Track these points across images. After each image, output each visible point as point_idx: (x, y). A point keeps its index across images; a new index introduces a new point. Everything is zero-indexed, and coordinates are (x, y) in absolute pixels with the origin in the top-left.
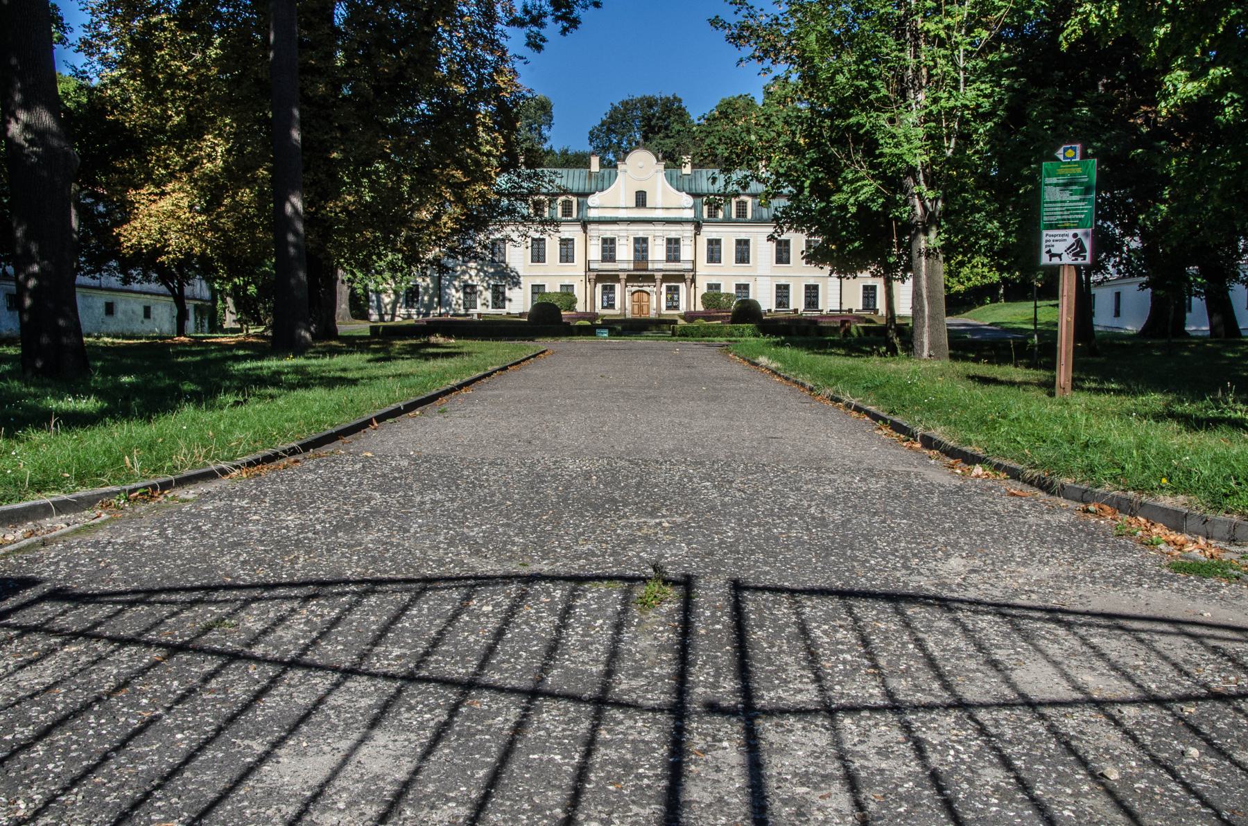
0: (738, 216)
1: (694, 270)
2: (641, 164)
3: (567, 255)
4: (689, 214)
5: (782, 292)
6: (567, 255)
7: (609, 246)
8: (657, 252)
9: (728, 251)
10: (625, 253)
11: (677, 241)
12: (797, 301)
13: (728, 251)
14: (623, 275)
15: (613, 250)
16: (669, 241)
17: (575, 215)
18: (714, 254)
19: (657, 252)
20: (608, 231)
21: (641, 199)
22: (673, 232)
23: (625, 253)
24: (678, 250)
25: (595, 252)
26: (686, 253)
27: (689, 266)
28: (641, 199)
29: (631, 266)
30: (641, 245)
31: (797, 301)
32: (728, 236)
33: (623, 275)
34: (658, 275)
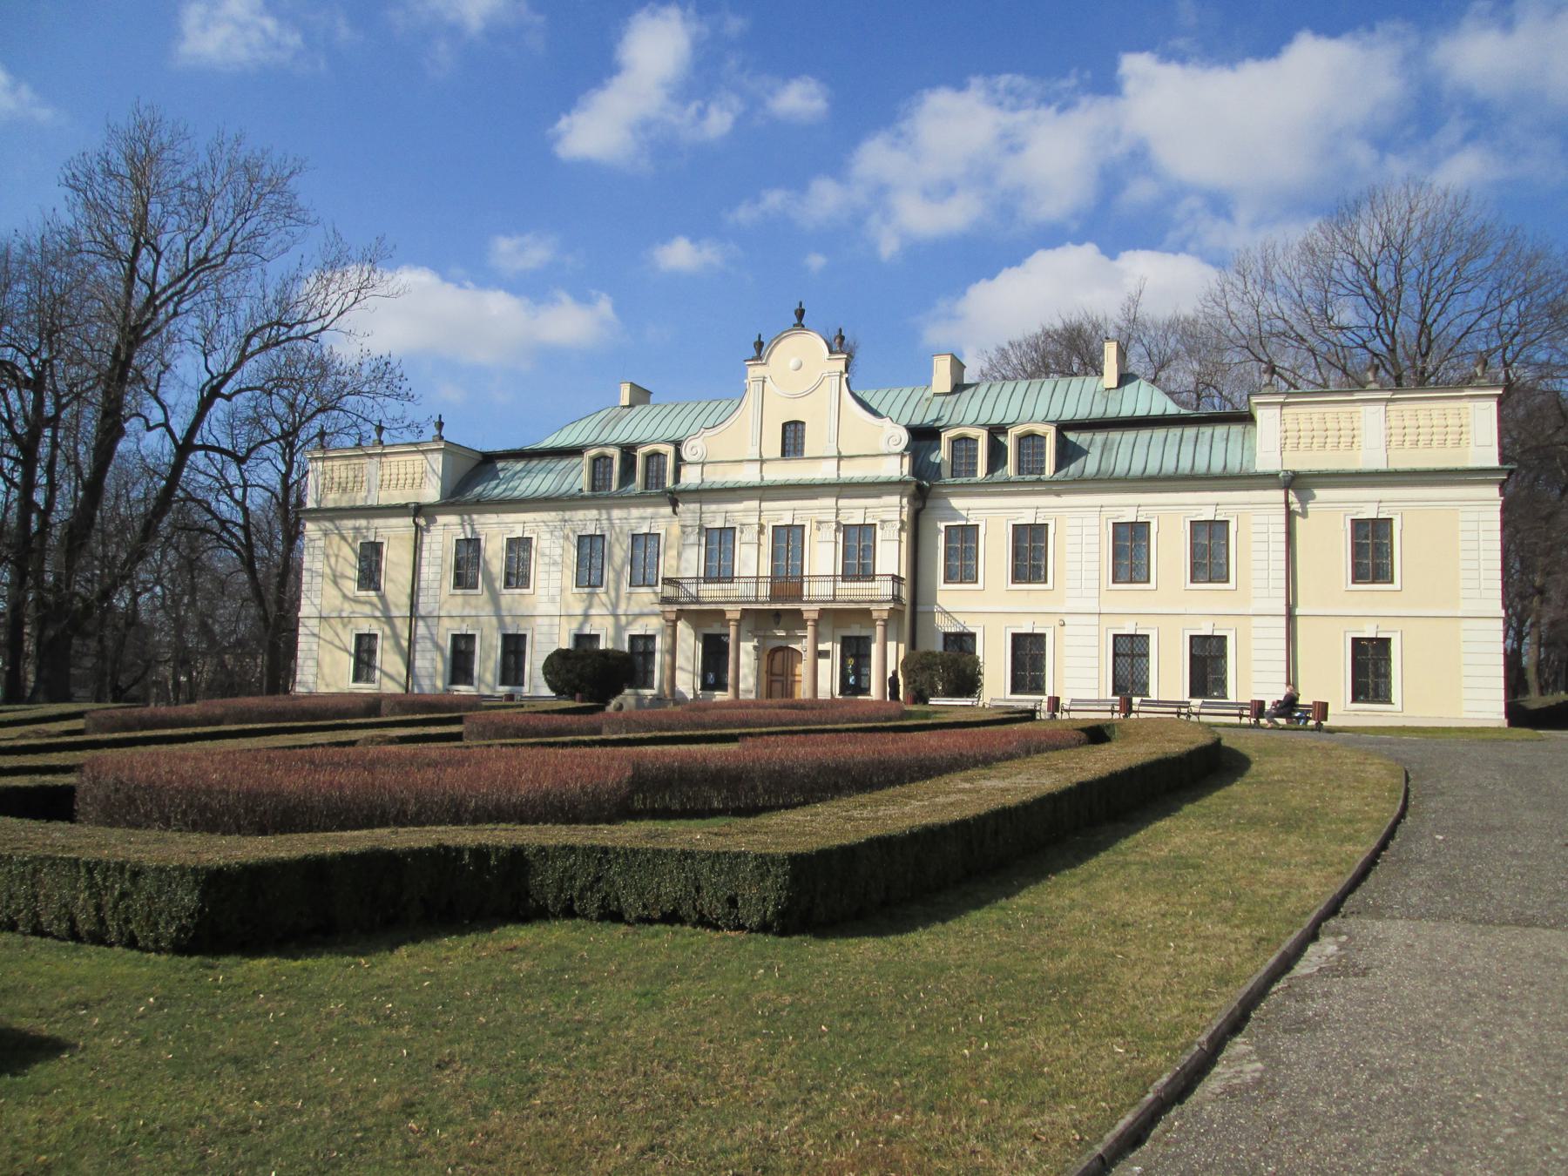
0: (1020, 470)
2: (793, 363)
5: (1130, 655)
7: (720, 542)
8: (821, 557)
9: (995, 553)
10: (752, 561)
11: (867, 530)
12: (1169, 677)
13: (995, 553)
14: (733, 612)
16: (846, 529)
17: (669, 483)
18: (963, 568)
19: (821, 557)
20: (716, 515)
21: (792, 438)
22: (855, 511)
23: (752, 561)
24: (869, 550)
28: (792, 438)
29: (765, 590)
30: (788, 540)
31: (1169, 677)
32: (993, 517)
33: (733, 612)
34: (810, 611)
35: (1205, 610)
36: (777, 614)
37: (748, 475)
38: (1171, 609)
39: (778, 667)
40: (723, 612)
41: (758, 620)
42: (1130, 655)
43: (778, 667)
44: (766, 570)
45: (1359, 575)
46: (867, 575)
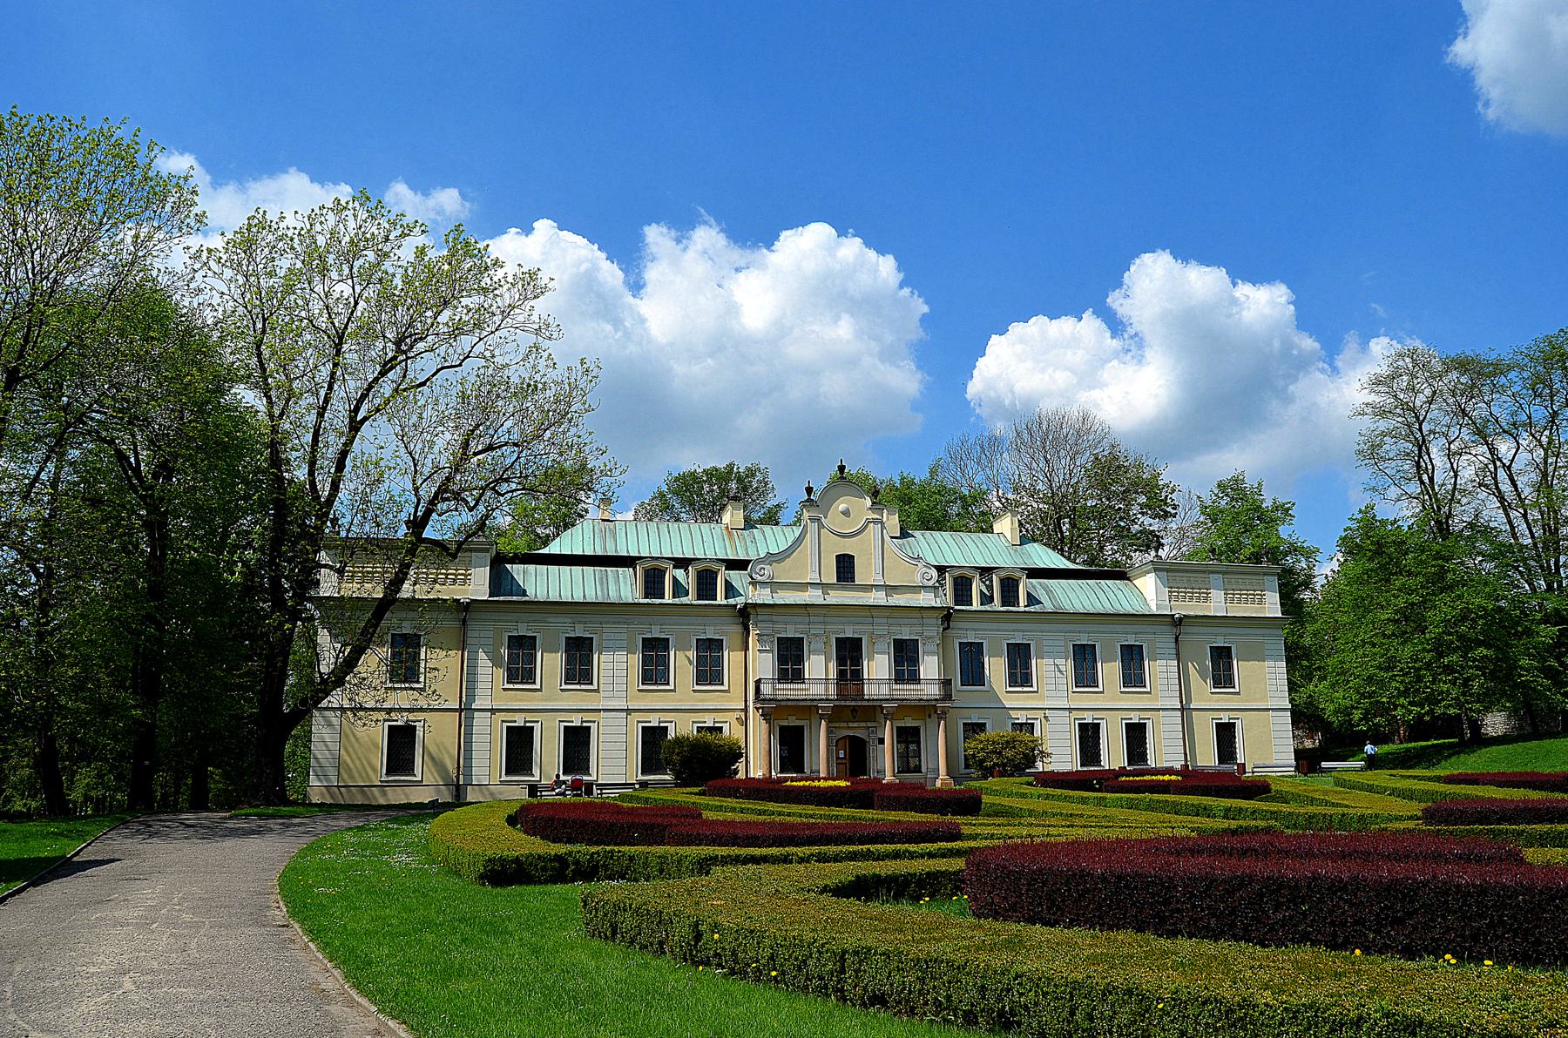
1: (947, 696)
2: (842, 507)
3: (709, 672)
4: (926, 599)
5: (1089, 736)
6: (709, 672)
10: (819, 668)
12: (1113, 755)
15: (800, 660)
17: (720, 599)
18: (973, 672)
19: (877, 667)
21: (845, 566)
23: (819, 668)
24: (915, 661)
25: (763, 663)
26: (929, 667)
27: (934, 691)
28: (845, 566)
29: (832, 690)
31: (1113, 755)
35: (1132, 703)
36: (854, 709)
37: (813, 596)
38: (1110, 702)
39: (855, 756)
40: (818, 708)
41: (837, 714)
42: (1089, 736)
43: (855, 756)
44: (833, 674)
45: (1217, 684)
46: (917, 681)
